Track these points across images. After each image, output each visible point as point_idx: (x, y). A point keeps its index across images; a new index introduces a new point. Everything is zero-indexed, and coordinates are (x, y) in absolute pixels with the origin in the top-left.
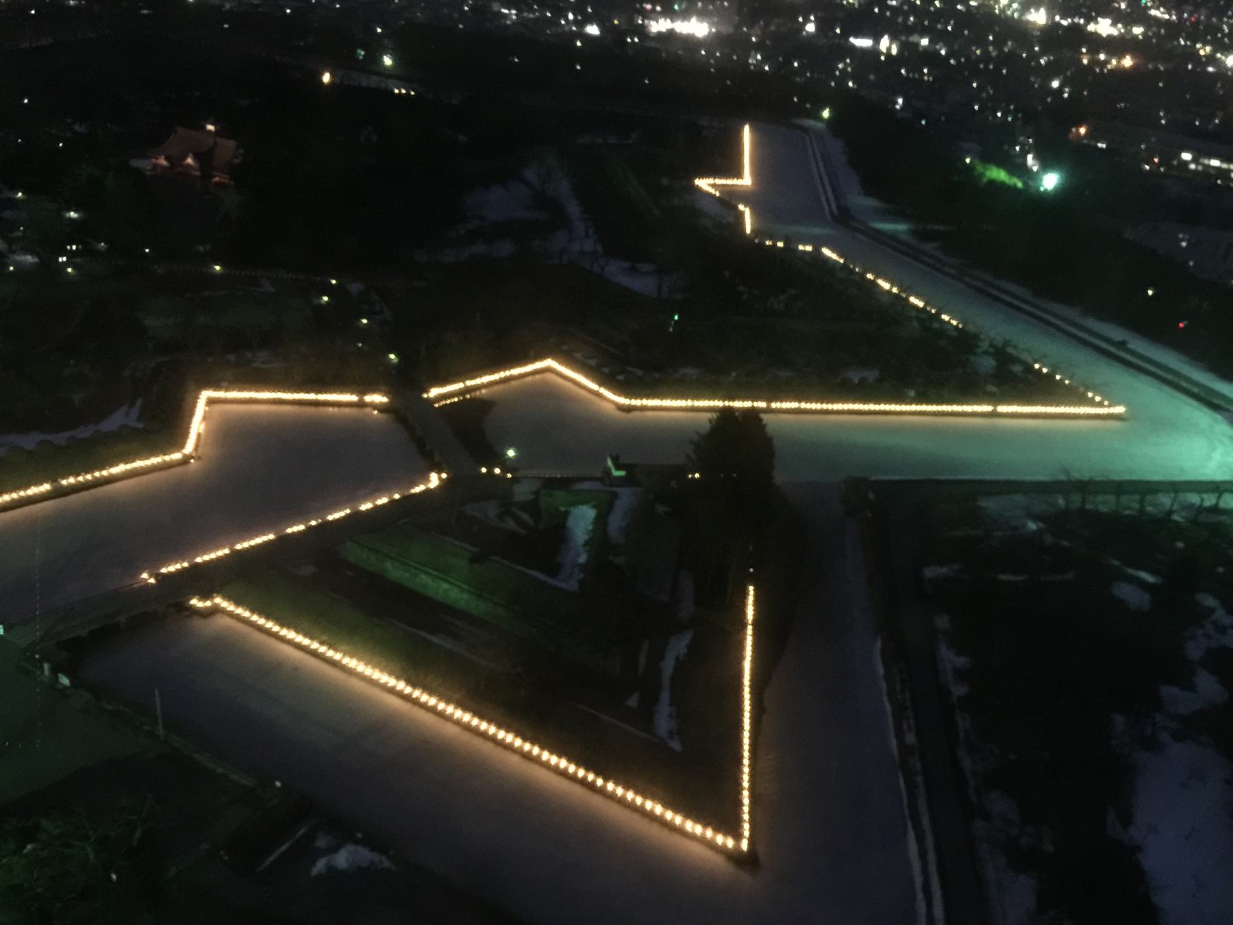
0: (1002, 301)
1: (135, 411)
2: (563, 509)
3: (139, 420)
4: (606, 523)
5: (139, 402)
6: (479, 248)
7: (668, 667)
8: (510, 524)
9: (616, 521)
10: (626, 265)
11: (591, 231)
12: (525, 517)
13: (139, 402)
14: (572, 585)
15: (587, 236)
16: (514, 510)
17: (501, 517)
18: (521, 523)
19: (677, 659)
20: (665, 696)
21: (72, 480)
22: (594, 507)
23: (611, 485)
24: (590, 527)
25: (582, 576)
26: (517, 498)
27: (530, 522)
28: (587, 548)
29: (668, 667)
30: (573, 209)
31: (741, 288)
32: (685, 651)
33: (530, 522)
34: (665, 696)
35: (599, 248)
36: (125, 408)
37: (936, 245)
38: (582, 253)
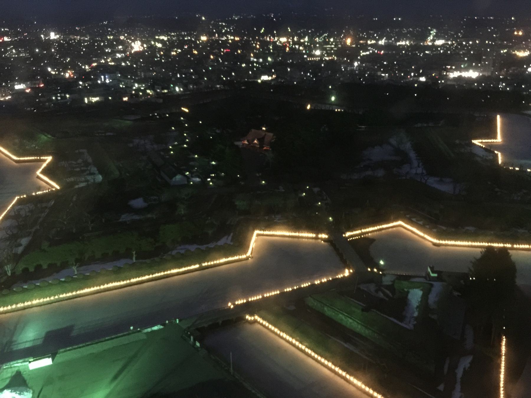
1: (230, 238)
2: (406, 290)
3: (232, 241)
6: (369, 173)
7: (460, 373)
8: (381, 295)
9: (432, 298)
10: (437, 179)
11: (421, 164)
12: (388, 292)
13: (232, 234)
15: (419, 166)
16: (383, 288)
17: (377, 291)
18: (387, 296)
19: (464, 369)
20: (458, 387)
22: (422, 290)
23: (430, 281)
24: (420, 300)
25: (415, 322)
27: (390, 295)
28: (418, 310)
29: (460, 373)
30: (412, 155)
31: (497, 189)
32: (469, 365)
33: (390, 295)
34: (458, 387)
35: (424, 172)
36: (226, 237)
38: (416, 174)
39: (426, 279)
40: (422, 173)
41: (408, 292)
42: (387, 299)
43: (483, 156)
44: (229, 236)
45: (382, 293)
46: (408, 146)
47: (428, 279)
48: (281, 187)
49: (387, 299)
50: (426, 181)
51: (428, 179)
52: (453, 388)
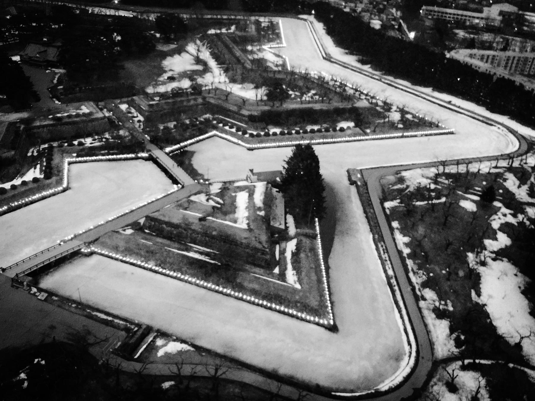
0: (399, 88)
2: (233, 194)
3: (40, 174)
4: (253, 199)
5: (38, 166)
7: (288, 255)
8: (212, 203)
13: (38, 166)
14: (245, 226)
16: (212, 197)
17: (207, 200)
18: (218, 203)
19: (292, 251)
20: (290, 266)
21: (16, 204)
23: (252, 182)
24: (247, 201)
26: (212, 192)
27: (221, 202)
28: (247, 210)
29: (288, 255)
32: (295, 248)
33: (221, 202)
34: (290, 266)
35: (227, 80)
36: (33, 169)
37: (369, 66)
39: (248, 182)
40: (225, 82)
41: (236, 196)
42: (219, 206)
43: (274, 61)
44: (35, 168)
45: (213, 200)
46: (206, 55)
47: (250, 181)
48: (83, 107)
49: (219, 206)
50: (231, 89)
51: (232, 87)
52: (286, 269)
